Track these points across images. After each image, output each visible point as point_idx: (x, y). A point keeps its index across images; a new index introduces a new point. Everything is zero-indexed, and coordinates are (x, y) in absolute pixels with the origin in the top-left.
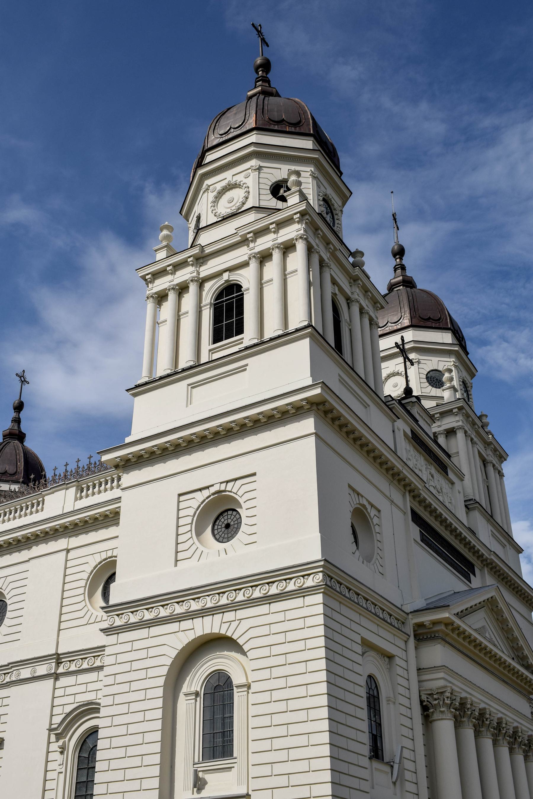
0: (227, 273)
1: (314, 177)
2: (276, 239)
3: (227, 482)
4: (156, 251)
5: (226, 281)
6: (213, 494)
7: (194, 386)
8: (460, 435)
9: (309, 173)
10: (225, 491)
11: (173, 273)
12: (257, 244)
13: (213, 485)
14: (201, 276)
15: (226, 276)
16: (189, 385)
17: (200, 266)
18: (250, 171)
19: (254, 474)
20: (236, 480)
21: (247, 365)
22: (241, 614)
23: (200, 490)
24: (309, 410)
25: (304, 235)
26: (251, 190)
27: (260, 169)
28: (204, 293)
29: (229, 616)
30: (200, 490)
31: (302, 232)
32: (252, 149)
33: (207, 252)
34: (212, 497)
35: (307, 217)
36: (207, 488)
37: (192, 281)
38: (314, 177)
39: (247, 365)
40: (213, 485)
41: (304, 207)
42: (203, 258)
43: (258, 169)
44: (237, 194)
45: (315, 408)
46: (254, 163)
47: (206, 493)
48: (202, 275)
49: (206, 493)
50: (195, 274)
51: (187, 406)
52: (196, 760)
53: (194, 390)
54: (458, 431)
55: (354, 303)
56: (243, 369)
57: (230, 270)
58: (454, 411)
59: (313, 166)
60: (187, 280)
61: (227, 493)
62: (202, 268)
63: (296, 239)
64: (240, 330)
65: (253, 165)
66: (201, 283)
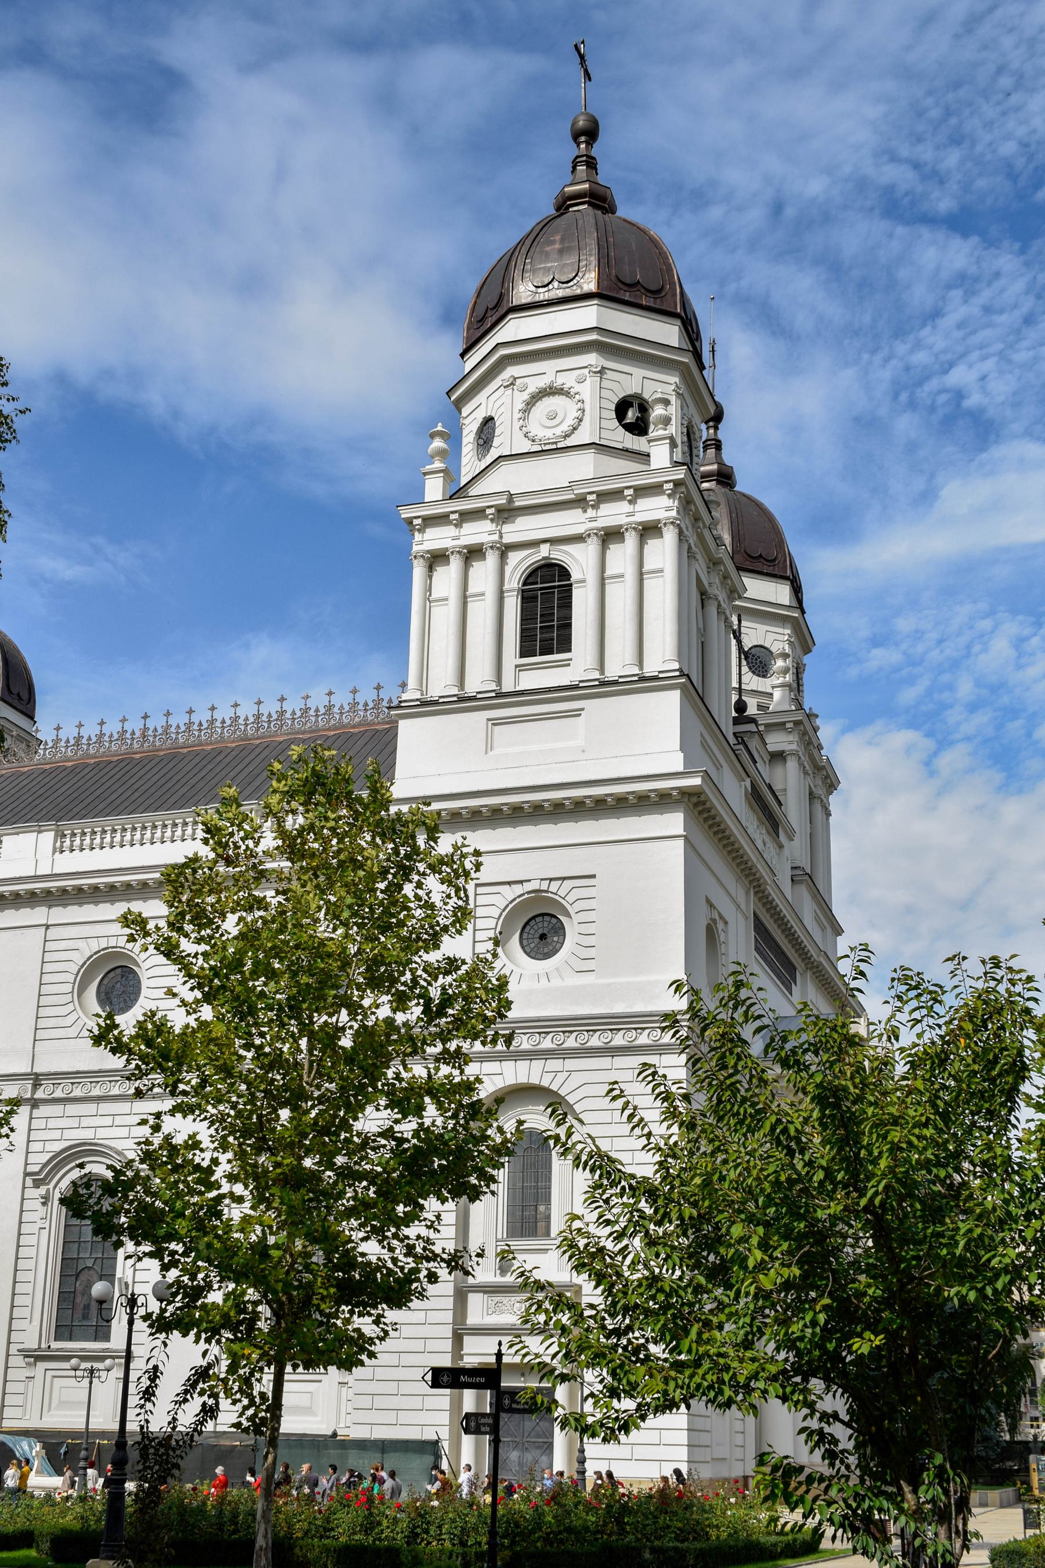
0: (548, 545)
1: (678, 393)
2: (631, 514)
3: (551, 880)
4: (425, 474)
5: (544, 558)
6: (529, 893)
7: (496, 722)
8: (792, 764)
9: (673, 387)
10: (547, 891)
11: (458, 525)
12: (600, 513)
13: (529, 881)
14: (504, 541)
15: (544, 550)
16: (489, 720)
17: (504, 523)
18: (586, 371)
19: (593, 876)
20: (564, 879)
21: (583, 709)
22: (571, 1064)
23: (509, 883)
24: (678, 802)
25: (676, 519)
26: (587, 407)
27: (602, 372)
28: (508, 570)
29: (554, 1064)
30: (509, 883)
31: (674, 513)
32: (594, 337)
33: (517, 504)
34: (526, 896)
35: (683, 489)
36: (521, 882)
37: (492, 547)
38: (678, 393)
39: (583, 709)
40: (529, 881)
41: (682, 476)
42: (509, 510)
43: (599, 372)
44: (564, 408)
45: (686, 799)
46: (592, 359)
47: (518, 889)
48: (507, 539)
49: (518, 889)
50: (496, 537)
51: (486, 753)
52: (499, 1236)
53: (497, 728)
54: (789, 758)
55: (711, 601)
56: (576, 713)
57: (553, 541)
58: (788, 725)
59: (678, 374)
60: (483, 544)
61: (550, 895)
62: (506, 528)
63: (665, 524)
64: (565, 644)
65: (593, 363)
66: (505, 550)
